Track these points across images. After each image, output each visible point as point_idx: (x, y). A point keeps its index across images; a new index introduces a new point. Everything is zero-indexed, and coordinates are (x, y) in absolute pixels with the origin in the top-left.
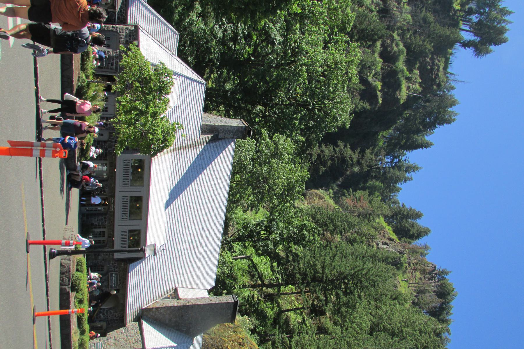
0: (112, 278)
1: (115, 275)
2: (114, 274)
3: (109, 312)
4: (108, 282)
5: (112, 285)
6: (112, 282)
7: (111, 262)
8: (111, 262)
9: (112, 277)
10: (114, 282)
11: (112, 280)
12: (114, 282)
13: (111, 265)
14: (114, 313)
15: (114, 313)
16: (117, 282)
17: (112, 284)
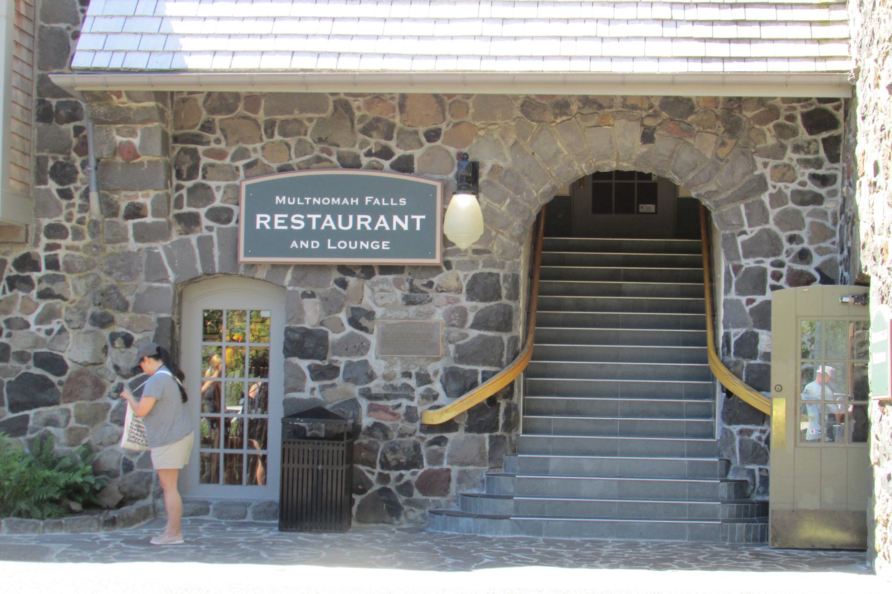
0: (307, 233)
1: (273, 210)
2: (262, 220)
3: (749, 263)
4: (368, 271)
5: (396, 236)
6: (355, 235)
7: (133, 245)
8: (133, 245)
9: (294, 235)
10: (363, 221)
11: (338, 235)
12: (363, 221)
13: (159, 247)
14: (759, 214)
15: (759, 214)
16: (359, 188)
17: (381, 235)
